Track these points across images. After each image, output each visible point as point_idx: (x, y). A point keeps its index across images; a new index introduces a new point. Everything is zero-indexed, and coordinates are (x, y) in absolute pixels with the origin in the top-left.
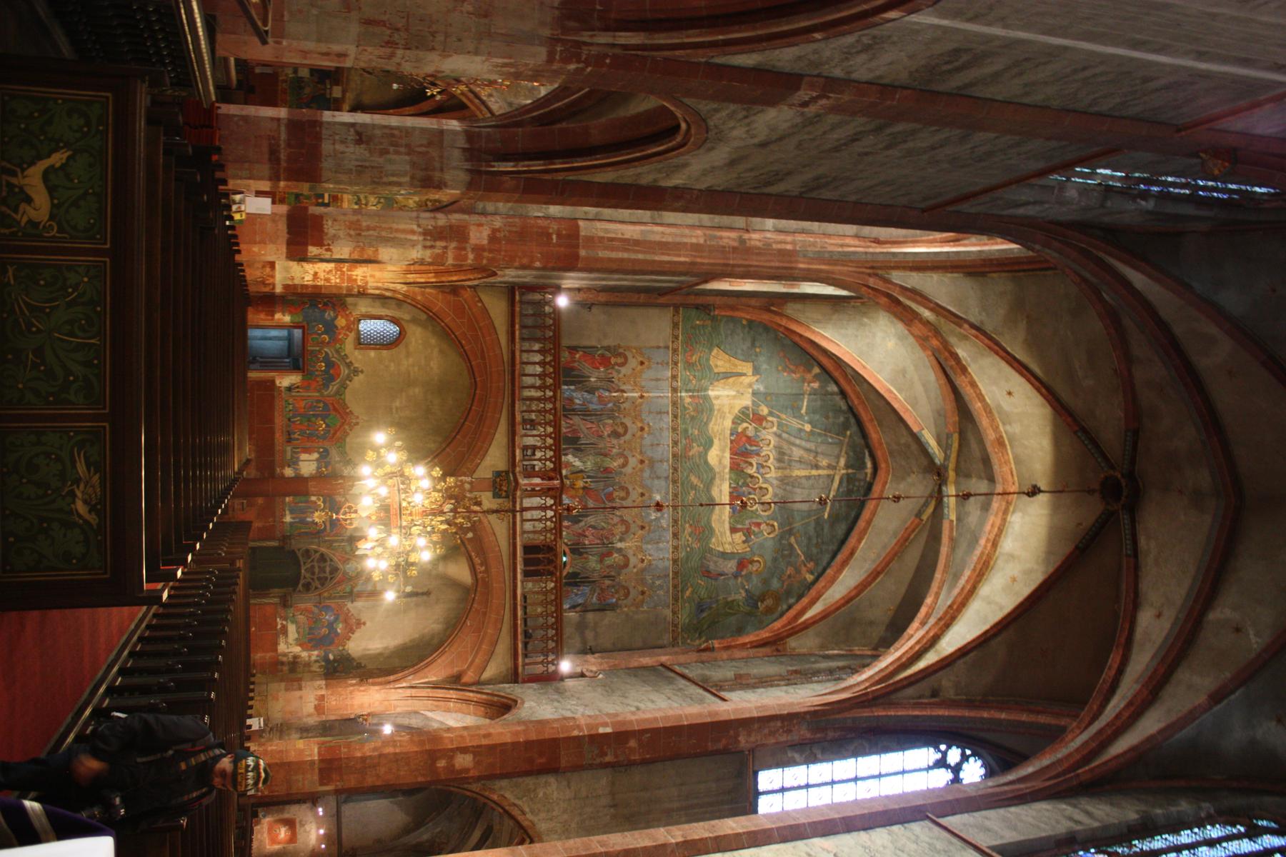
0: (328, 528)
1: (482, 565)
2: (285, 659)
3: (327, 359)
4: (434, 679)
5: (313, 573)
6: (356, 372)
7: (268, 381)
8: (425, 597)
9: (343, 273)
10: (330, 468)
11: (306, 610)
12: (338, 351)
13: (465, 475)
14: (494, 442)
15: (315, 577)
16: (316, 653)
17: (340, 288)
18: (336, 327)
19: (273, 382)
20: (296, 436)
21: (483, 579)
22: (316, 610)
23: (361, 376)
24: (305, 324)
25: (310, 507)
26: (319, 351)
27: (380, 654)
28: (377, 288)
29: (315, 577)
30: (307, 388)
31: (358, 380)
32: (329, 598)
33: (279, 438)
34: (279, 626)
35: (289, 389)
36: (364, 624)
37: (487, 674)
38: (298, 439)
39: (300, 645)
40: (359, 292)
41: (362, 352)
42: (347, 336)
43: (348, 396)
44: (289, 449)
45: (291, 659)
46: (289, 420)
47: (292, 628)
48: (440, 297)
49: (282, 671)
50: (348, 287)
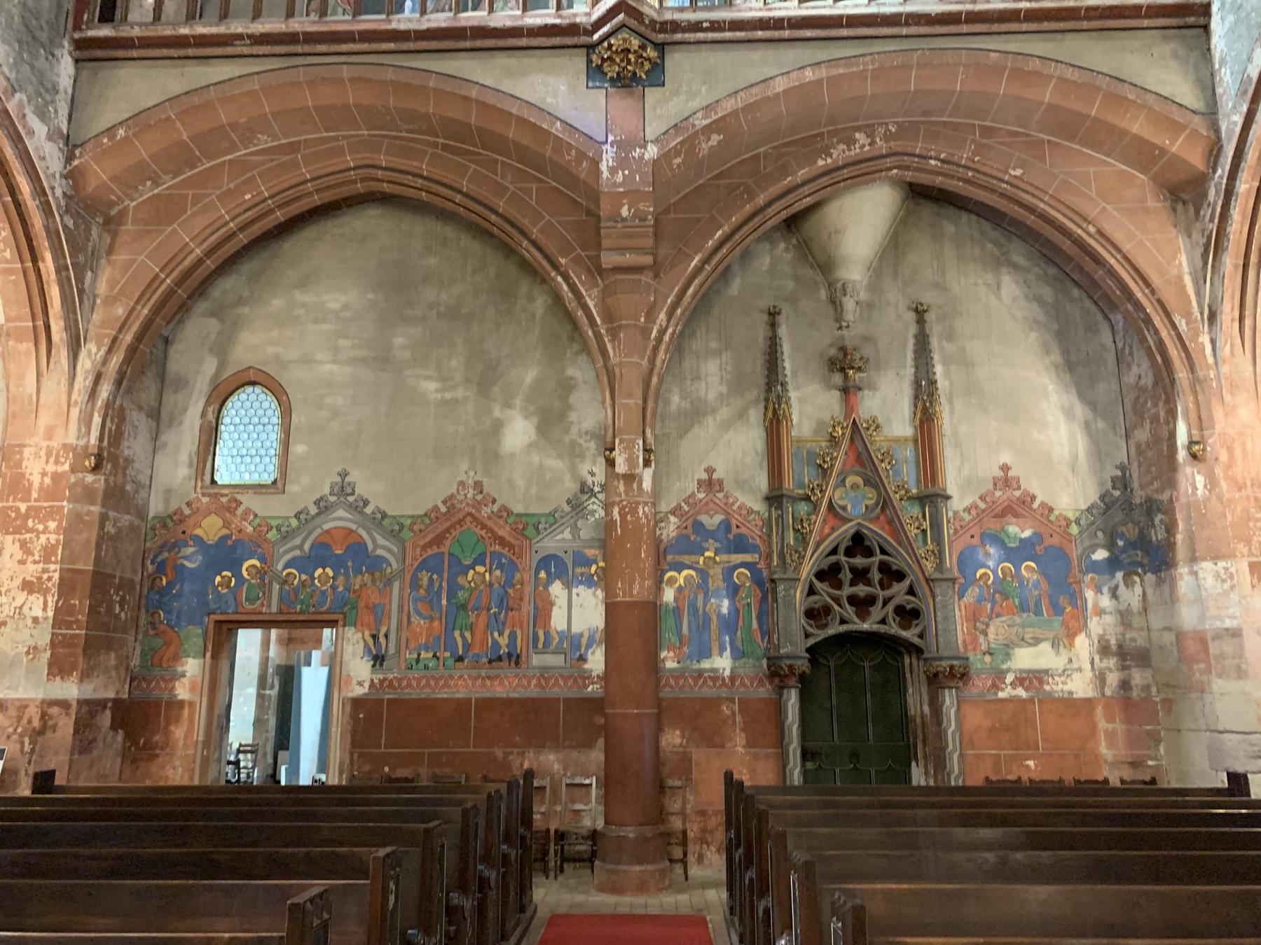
0: (747, 558)
1: (850, 142)
2: (1113, 679)
3: (306, 563)
4: (1183, 258)
5: (870, 600)
6: (343, 489)
7: (354, 716)
8: (930, 317)
9: (33, 512)
10: (590, 552)
11: (974, 617)
12: (287, 536)
13: (595, 163)
14: (507, 86)
15: (882, 594)
16: (1089, 595)
17: (77, 519)
18: (224, 539)
19: (357, 703)
20: (503, 641)
21: (887, 137)
22: (972, 594)
23: (355, 476)
24: (209, 621)
25: (693, 606)
26: (284, 582)
27: (1087, 425)
28: (86, 421)
29: (882, 594)
30: (378, 613)
31: (365, 485)
32: (940, 556)
33: (506, 686)
34: (1021, 692)
35: (378, 660)
36: (1005, 468)
37: (1185, 92)
38: (513, 637)
39: (1071, 636)
40: (96, 468)
41: (291, 475)
42: (248, 511)
43: (408, 507)
44: (536, 660)
45: (1112, 662)
46: (460, 659)
47: (1025, 658)
48: (120, 257)
49: (1146, 688)
50: (73, 499)
